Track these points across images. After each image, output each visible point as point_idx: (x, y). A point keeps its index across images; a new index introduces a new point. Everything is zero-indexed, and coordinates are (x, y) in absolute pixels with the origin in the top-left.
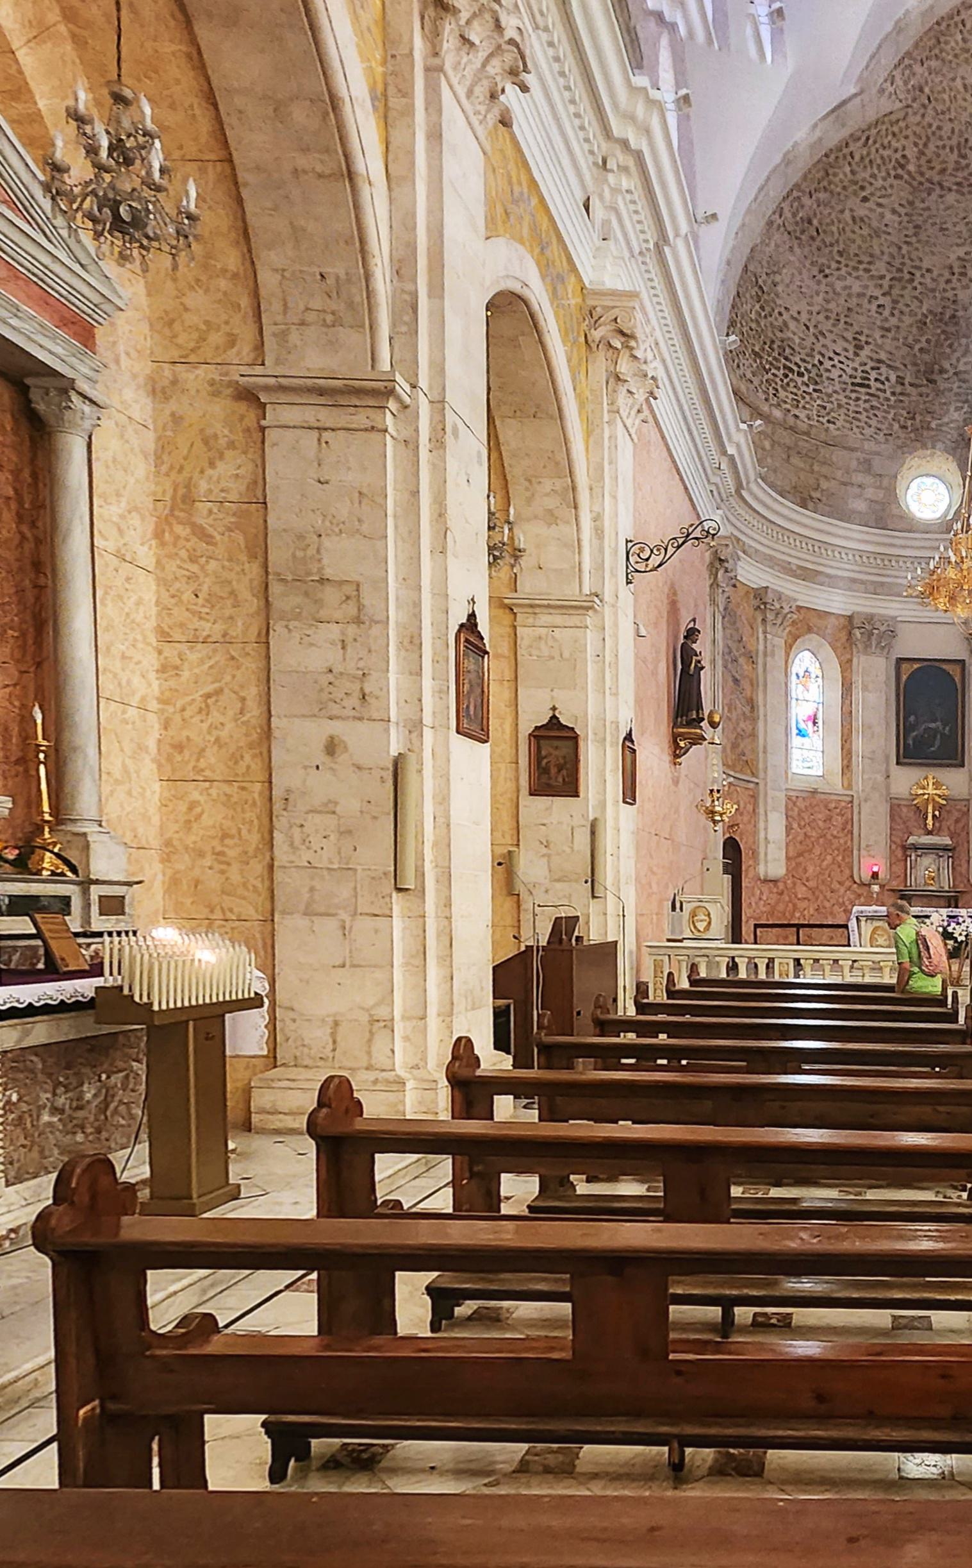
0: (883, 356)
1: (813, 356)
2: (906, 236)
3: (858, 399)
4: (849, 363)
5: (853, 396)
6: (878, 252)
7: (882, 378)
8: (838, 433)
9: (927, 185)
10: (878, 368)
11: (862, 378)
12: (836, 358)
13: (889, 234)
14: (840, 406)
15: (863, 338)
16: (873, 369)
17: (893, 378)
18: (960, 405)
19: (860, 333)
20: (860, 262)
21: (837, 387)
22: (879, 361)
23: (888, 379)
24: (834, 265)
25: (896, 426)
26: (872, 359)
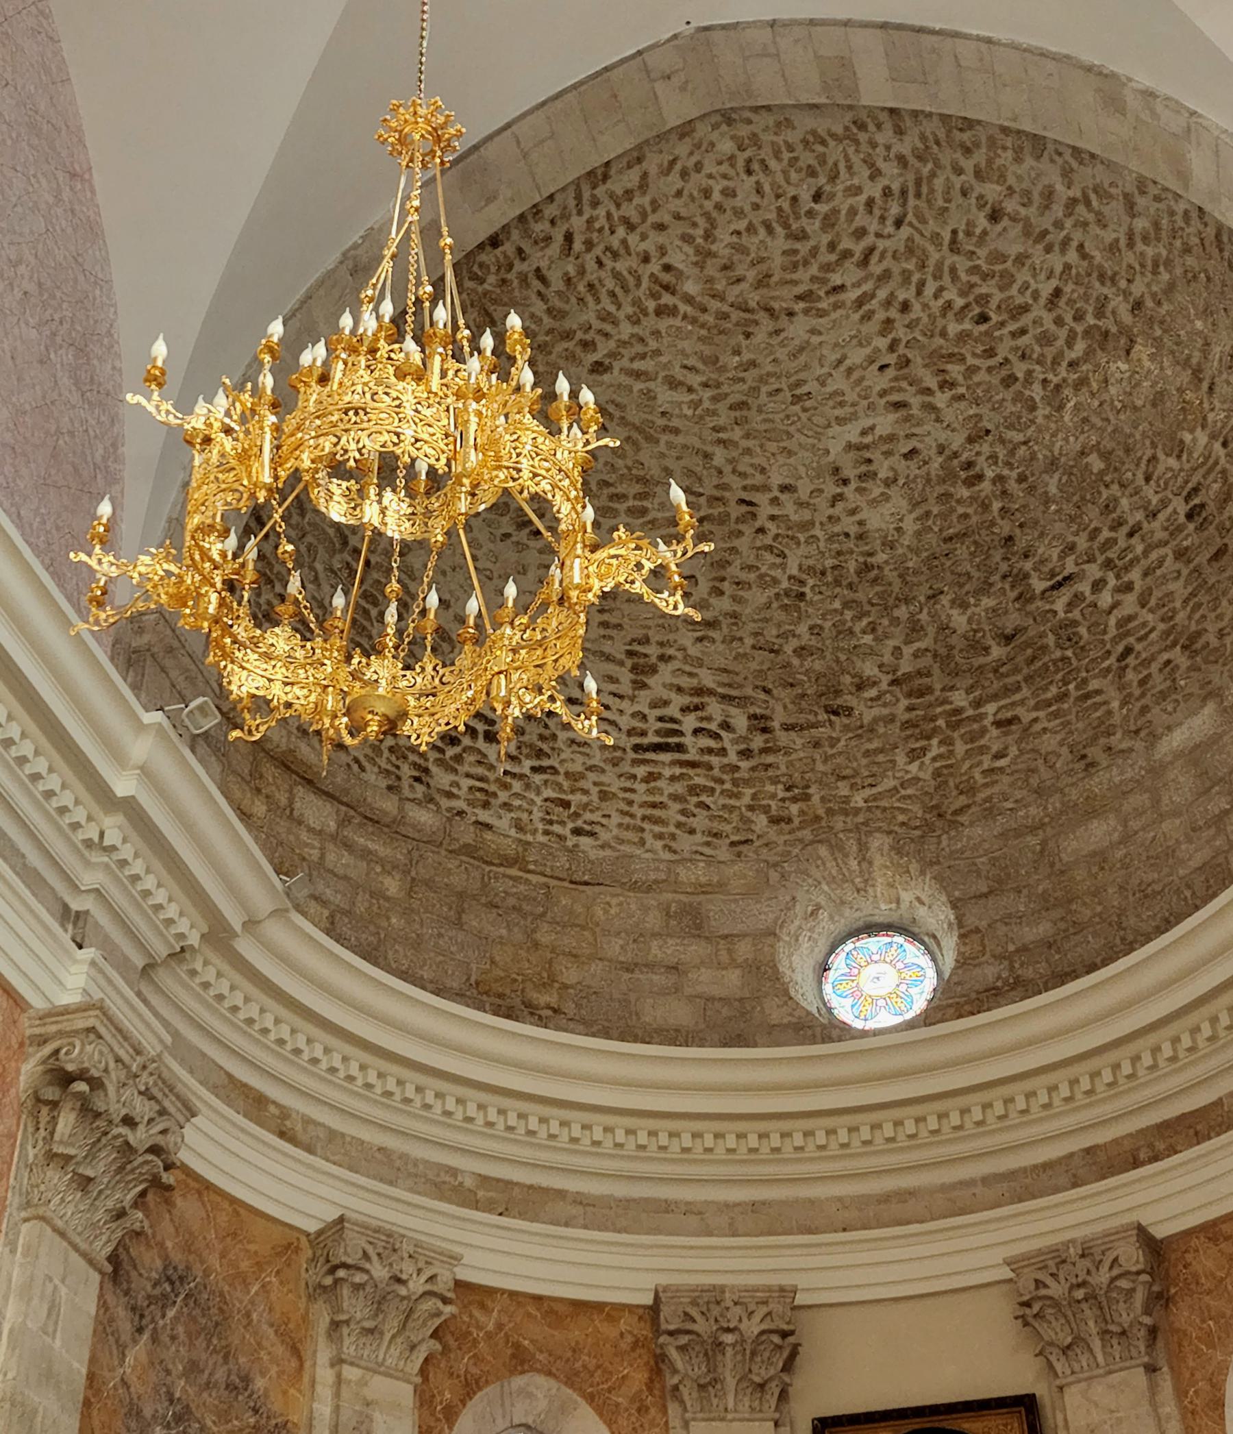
0: (708, 679)
2: (716, 429)
3: (651, 777)
4: (625, 705)
5: (641, 771)
6: (656, 472)
7: (713, 726)
8: (602, 853)
9: (736, 315)
10: (696, 708)
11: (658, 733)
13: (676, 431)
14: (604, 796)
15: (653, 651)
16: (685, 710)
17: (740, 722)
19: (645, 641)
20: (620, 497)
21: (597, 759)
22: (700, 691)
23: (726, 726)
26: (679, 689)
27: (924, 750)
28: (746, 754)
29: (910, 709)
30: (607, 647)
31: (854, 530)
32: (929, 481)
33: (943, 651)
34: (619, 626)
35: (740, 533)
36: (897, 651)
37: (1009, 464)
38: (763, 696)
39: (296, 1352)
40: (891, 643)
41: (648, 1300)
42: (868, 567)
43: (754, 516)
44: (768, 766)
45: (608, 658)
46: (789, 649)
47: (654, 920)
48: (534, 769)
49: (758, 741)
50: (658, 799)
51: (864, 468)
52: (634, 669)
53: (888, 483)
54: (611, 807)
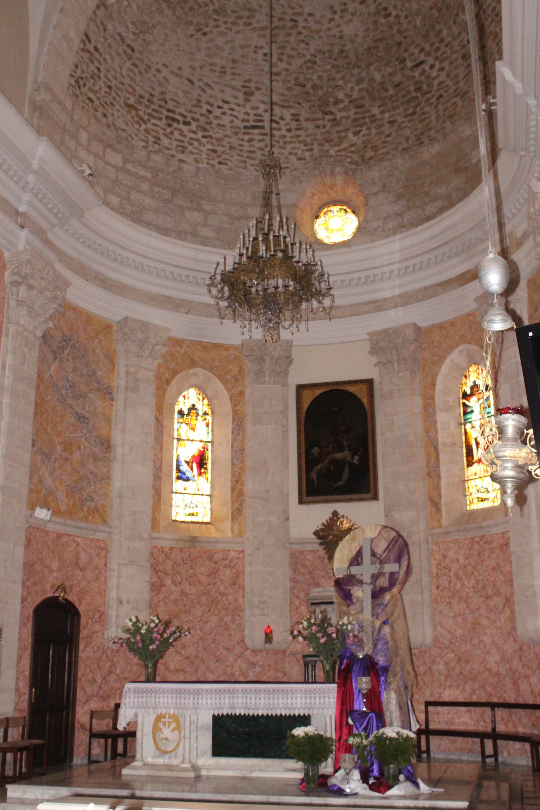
1: (201, 107)
3: (250, 140)
4: (241, 109)
5: (247, 137)
8: (229, 172)
11: (255, 121)
12: (226, 106)
14: (231, 148)
15: (253, 85)
17: (288, 117)
19: (250, 81)
21: (229, 132)
23: (282, 118)
24: (212, 23)
27: (359, 132)
28: (289, 130)
29: (356, 113)
30: (234, 83)
31: (338, 34)
32: (369, 15)
33: (370, 90)
34: (239, 75)
35: (289, 34)
36: (352, 88)
37: (401, 10)
38: (297, 106)
39: (112, 363)
40: (350, 85)
42: (343, 51)
43: (296, 26)
44: (298, 136)
45: (234, 88)
46: (309, 86)
47: (249, 199)
48: (204, 137)
49: (294, 125)
50: (252, 149)
51: (343, 7)
52: (245, 93)
53: (353, 14)
54: (233, 153)
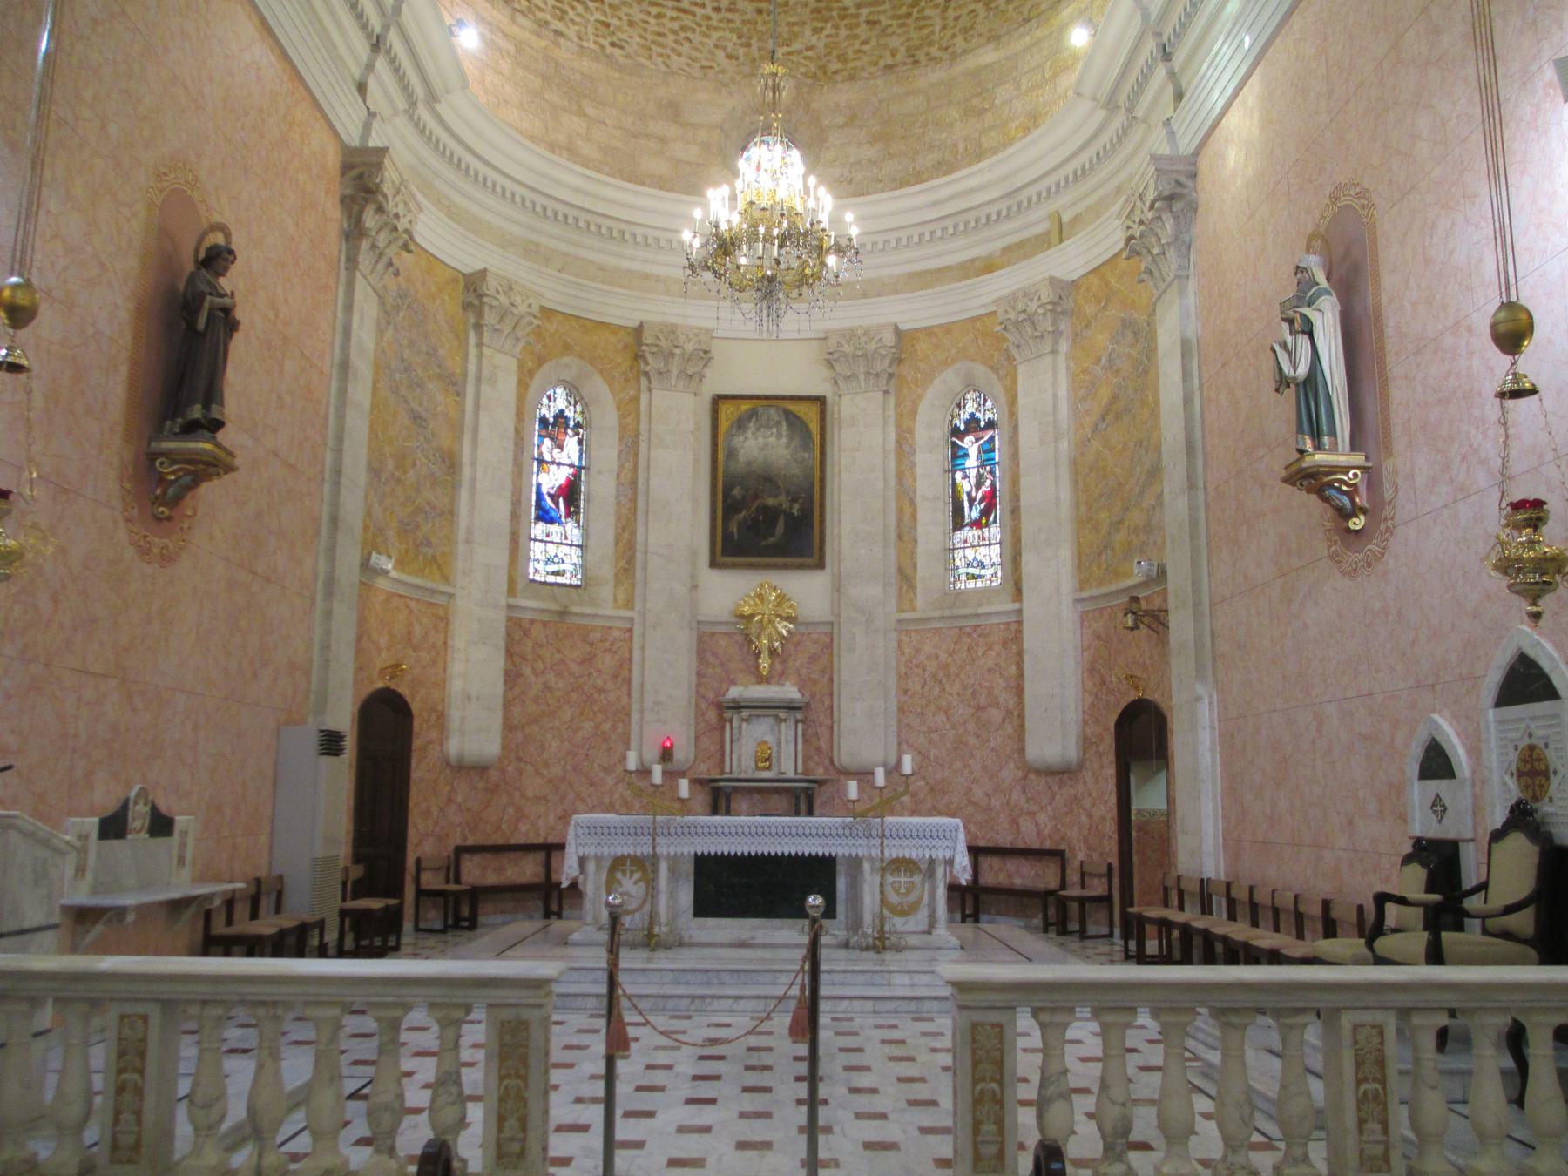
18: (820, 25)
25: (720, 54)
41: (636, 324)
